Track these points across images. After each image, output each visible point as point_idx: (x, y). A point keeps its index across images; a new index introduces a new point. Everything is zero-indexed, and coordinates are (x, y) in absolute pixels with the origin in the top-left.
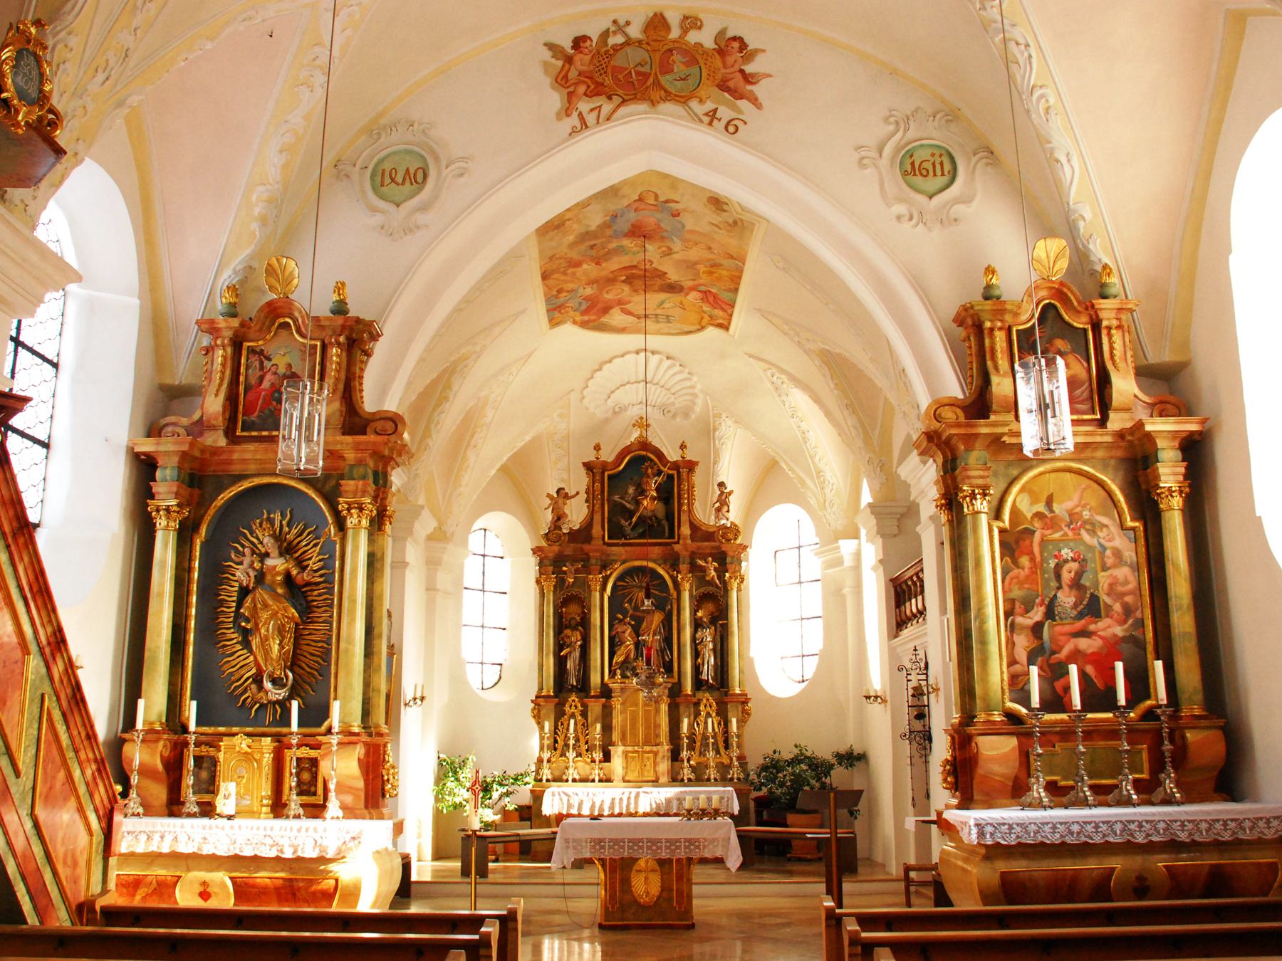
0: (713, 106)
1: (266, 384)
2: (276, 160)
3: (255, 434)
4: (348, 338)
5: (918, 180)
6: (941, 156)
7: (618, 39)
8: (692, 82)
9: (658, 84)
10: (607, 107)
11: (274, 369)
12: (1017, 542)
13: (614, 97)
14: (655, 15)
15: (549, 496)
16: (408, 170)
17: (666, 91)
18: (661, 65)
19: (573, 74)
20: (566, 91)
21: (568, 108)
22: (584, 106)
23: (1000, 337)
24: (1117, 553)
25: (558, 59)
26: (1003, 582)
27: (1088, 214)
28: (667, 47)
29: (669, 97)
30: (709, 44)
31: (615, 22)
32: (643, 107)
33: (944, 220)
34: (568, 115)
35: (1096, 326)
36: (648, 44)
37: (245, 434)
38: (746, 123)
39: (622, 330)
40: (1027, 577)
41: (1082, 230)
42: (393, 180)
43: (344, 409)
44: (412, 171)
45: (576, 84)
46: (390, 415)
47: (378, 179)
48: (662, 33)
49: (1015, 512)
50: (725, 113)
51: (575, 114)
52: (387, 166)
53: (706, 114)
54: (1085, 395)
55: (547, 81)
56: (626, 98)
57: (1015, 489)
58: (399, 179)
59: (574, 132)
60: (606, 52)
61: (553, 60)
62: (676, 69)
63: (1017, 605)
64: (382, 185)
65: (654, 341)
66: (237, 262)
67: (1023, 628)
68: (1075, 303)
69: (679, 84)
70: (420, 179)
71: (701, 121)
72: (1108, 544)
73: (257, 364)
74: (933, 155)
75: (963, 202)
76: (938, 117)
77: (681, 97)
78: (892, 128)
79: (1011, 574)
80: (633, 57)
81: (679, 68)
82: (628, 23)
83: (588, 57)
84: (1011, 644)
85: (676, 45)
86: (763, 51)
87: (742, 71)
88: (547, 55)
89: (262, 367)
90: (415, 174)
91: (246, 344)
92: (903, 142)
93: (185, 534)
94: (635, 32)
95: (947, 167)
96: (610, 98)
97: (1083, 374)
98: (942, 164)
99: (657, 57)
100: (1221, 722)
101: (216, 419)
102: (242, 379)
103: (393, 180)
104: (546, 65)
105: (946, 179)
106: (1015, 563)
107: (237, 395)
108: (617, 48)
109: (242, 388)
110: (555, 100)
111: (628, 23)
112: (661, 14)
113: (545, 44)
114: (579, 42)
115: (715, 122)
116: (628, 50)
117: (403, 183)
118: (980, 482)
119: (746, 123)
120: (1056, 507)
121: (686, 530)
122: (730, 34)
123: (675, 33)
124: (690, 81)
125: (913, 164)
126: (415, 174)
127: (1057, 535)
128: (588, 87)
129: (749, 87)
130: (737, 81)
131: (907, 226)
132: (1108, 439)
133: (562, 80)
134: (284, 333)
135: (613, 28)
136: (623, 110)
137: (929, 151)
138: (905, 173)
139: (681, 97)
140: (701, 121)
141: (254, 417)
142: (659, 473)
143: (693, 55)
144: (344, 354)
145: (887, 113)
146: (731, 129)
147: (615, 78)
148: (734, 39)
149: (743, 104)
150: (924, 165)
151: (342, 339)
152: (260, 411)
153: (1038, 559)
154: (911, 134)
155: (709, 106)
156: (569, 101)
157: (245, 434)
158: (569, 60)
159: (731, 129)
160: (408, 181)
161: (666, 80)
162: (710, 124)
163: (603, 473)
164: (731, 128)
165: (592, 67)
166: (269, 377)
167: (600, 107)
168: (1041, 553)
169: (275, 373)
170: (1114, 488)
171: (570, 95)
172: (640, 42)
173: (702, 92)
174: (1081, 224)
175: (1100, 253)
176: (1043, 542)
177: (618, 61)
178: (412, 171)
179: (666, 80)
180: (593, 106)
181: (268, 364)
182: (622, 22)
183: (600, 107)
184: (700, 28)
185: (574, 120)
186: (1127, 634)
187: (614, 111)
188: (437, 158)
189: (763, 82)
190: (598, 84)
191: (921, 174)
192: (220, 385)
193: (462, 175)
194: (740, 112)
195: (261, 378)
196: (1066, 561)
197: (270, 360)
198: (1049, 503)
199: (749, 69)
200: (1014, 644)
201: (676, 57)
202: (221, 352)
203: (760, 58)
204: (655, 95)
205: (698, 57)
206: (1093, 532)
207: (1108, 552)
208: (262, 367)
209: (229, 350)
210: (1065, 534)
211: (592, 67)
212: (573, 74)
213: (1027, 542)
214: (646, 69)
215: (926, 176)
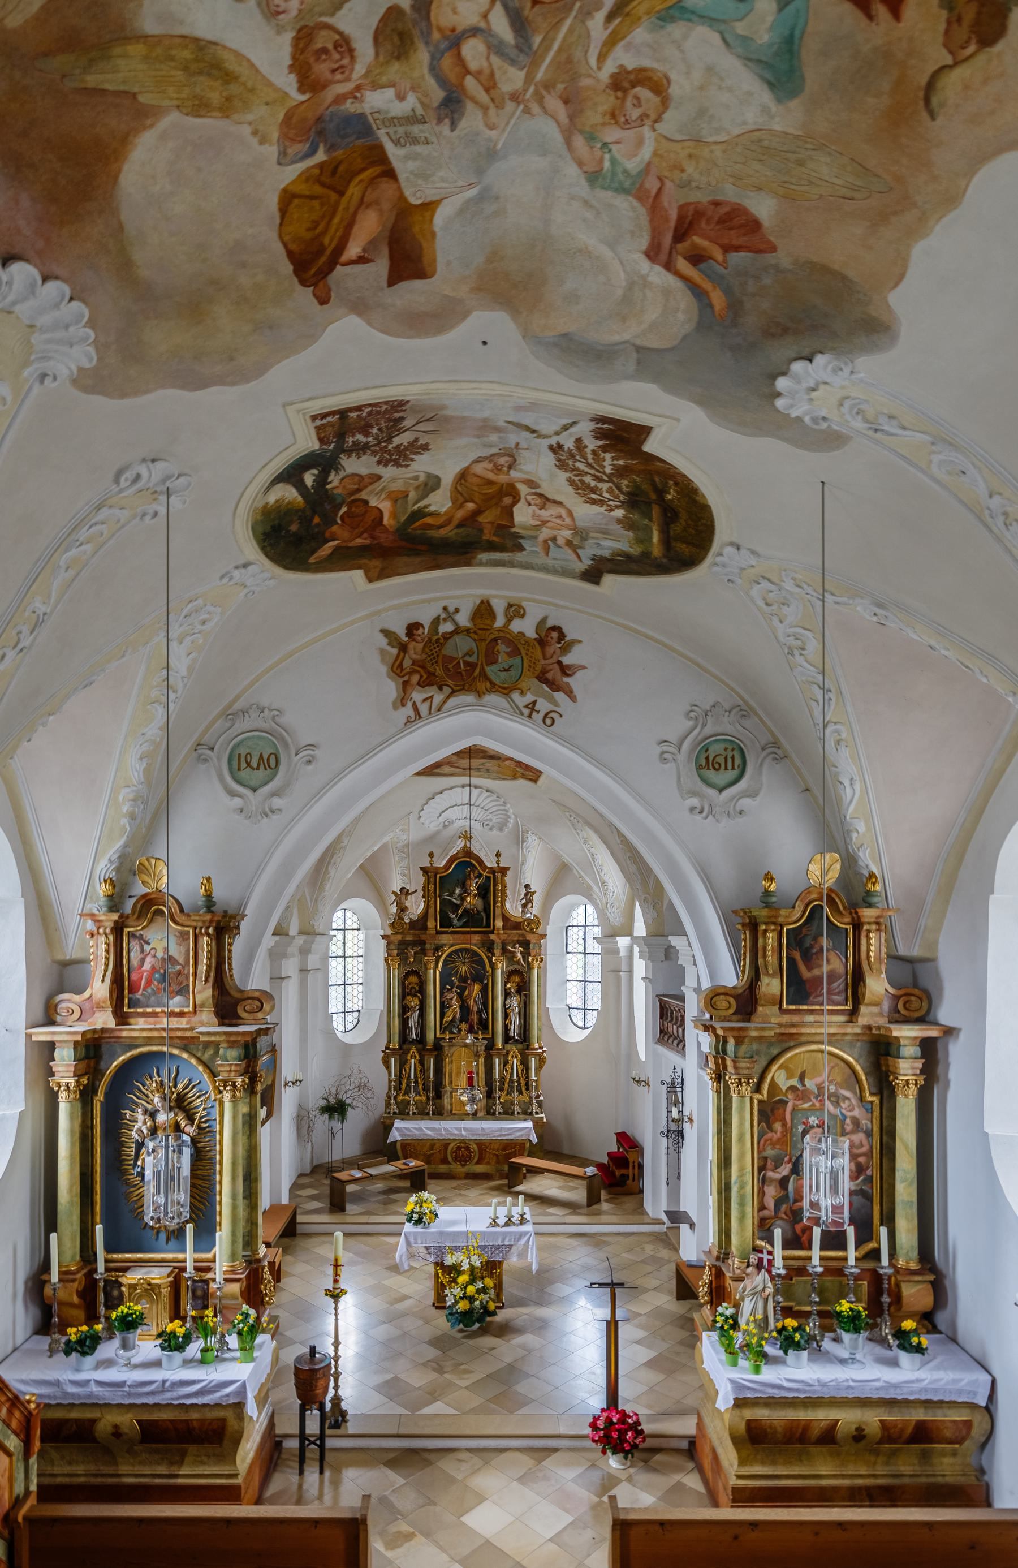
0: (533, 699)
1: (147, 966)
2: (137, 766)
3: (140, 1010)
4: (216, 929)
5: (711, 774)
6: (733, 750)
7: (446, 627)
8: (514, 673)
9: (483, 675)
10: (438, 698)
11: (152, 952)
12: (772, 1111)
13: (445, 688)
14: (482, 602)
15: (393, 892)
16: (261, 755)
17: (491, 683)
18: (487, 656)
19: (407, 663)
20: (401, 680)
21: (403, 698)
22: (417, 696)
23: (771, 937)
24: (856, 1122)
25: (393, 647)
26: (759, 1143)
27: (861, 827)
28: (492, 636)
29: (494, 688)
30: (531, 633)
31: (445, 609)
32: (469, 698)
33: (731, 811)
34: (403, 705)
35: (857, 926)
36: (475, 633)
37: (132, 1010)
38: (561, 716)
39: (452, 775)
40: (779, 1139)
41: (854, 839)
42: (248, 764)
43: (216, 993)
44: (265, 757)
45: (410, 673)
46: (257, 994)
47: (235, 763)
48: (488, 622)
49: (773, 1085)
50: (543, 705)
51: (410, 704)
52: (243, 751)
53: (526, 706)
54: (842, 987)
55: (384, 669)
56: (455, 688)
57: (774, 1068)
58: (254, 764)
59: (409, 722)
60: (438, 640)
61: (389, 648)
62: (500, 660)
63: (769, 1162)
64: (239, 769)
65: (475, 781)
66: (111, 853)
67: (772, 1180)
68: (841, 908)
69: (503, 675)
70: (273, 763)
71: (522, 714)
72: (849, 1114)
73: (137, 947)
74: (726, 749)
75: (749, 796)
76: (733, 713)
77: (505, 688)
78: (691, 723)
79: (765, 1137)
80: (461, 646)
81: (503, 659)
82: (457, 610)
83: (421, 645)
84: (762, 1193)
85: (502, 634)
86: (580, 642)
87: (559, 663)
88: (383, 642)
89: (142, 951)
90: (268, 759)
91: (126, 930)
92: (700, 738)
93: (85, 1095)
94: (463, 619)
95: (738, 761)
96: (440, 688)
97: (841, 969)
98: (733, 758)
99: (484, 644)
100: (932, 1277)
101: (104, 1002)
102: (125, 961)
103: (248, 764)
104: (382, 652)
105: (735, 773)
106: (770, 1128)
107: (122, 975)
108: (448, 636)
109: (125, 970)
110: (391, 689)
111: (457, 610)
112: (488, 602)
113: (382, 631)
114: (412, 628)
115: (534, 714)
116: (457, 638)
117: (258, 768)
118: (746, 1072)
119: (561, 716)
120: (807, 1081)
121: (499, 923)
122: (550, 623)
123: (500, 622)
124: (513, 673)
125: (707, 758)
126: (268, 759)
127: (806, 1106)
128: (421, 676)
129: (566, 679)
130: (554, 673)
131: (699, 818)
132: (858, 1030)
133: (397, 669)
134: (159, 919)
135: (443, 616)
136: (453, 701)
137: (723, 746)
138: (699, 768)
139: (505, 688)
140: (522, 714)
141: (138, 995)
142: (480, 876)
143: (516, 644)
144: (214, 944)
145: (690, 708)
146: (548, 721)
147: (446, 668)
148: (554, 628)
149: (560, 696)
150: (718, 759)
151: (211, 931)
152: (144, 990)
153: (789, 1124)
154: (708, 730)
155: (529, 698)
156: (404, 691)
157: (132, 1010)
158: (403, 648)
159: (548, 721)
160: (262, 766)
161: (490, 670)
162: (530, 716)
163: (435, 877)
164: (549, 720)
165: (424, 656)
166: (149, 960)
167: (432, 697)
168: (792, 1120)
169: (154, 956)
170: (858, 1068)
171: (405, 684)
172: (467, 631)
173: (523, 684)
174: (854, 835)
175: (868, 861)
176: (794, 1110)
177: (448, 650)
178: (265, 757)
179: (490, 670)
180: (426, 696)
181: (147, 948)
182: (451, 609)
183: (432, 697)
184: (523, 616)
185: (408, 710)
186: (858, 1188)
187: (444, 702)
188: (286, 745)
189: (579, 674)
190: (431, 674)
191: (714, 768)
192: (106, 971)
193: (309, 762)
194: (556, 704)
195: (143, 960)
196: (812, 1127)
197: (149, 944)
198: (802, 1078)
199: (566, 660)
200: (764, 1193)
201: (501, 647)
202: (104, 939)
203: (576, 649)
204: (482, 686)
205: (521, 647)
206: (837, 1104)
207: (848, 1121)
208: (142, 951)
209: (111, 938)
210: (813, 1105)
211: (424, 656)
212: (407, 663)
213: (781, 1111)
214: (472, 659)
215: (717, 770)
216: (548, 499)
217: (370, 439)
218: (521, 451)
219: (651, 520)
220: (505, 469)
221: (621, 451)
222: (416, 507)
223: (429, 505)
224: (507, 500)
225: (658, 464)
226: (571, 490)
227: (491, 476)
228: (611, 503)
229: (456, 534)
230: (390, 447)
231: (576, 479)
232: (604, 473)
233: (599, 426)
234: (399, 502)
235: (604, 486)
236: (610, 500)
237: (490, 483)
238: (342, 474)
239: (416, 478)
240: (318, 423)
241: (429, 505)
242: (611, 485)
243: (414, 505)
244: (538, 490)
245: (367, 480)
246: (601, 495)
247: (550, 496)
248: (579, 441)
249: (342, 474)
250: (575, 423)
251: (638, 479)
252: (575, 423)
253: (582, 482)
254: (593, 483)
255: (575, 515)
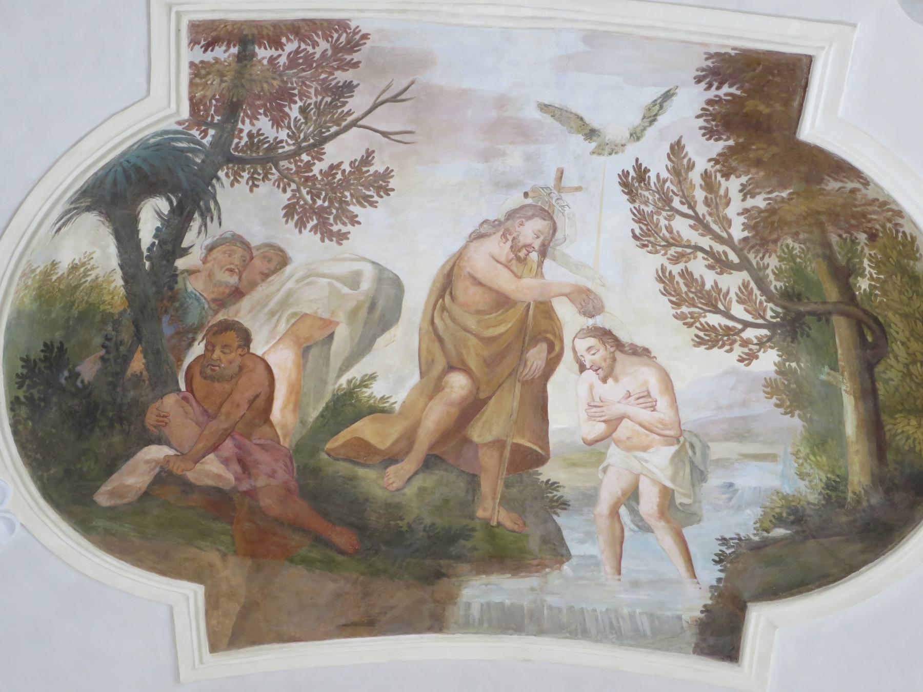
216: (618, 344)
217: (283, 134)
218: (567, 198)
219: (834, 367)
220: (534, 256)
221: (758, 163)
222: (343, 381)
223: (372, 377)
224: (536, 356)
225: (832, 185)
226: (664, 306)
227: (504, 281)
228: (750, 334)
229: (422, 491)
230: (318, 168)
231: (676, 269)
232: (729, 242)
233: (712, 94)
234: (314, 352)
235: (732, 282)
236: (746, 324)
237: (503, 302)
238: (215, 231)
239: (353, 280)
240: (198, 55)
241: (372, 377)
242: (745, 275)
243: (342, 371)
244: (599, 321)
245: (259, 264)
246: (728, 315)
247: (624, 337)
248: (677, 149)
249: (215, 231)
250: (668, 96)
251: (797, 248)
252: (668, 96)
253: (686, 275)
254: (710, 278)
255: (678, 386)
